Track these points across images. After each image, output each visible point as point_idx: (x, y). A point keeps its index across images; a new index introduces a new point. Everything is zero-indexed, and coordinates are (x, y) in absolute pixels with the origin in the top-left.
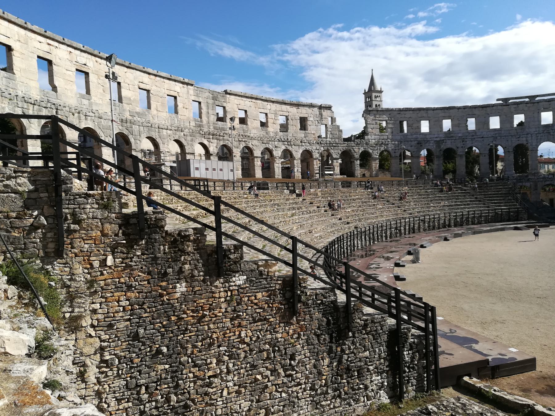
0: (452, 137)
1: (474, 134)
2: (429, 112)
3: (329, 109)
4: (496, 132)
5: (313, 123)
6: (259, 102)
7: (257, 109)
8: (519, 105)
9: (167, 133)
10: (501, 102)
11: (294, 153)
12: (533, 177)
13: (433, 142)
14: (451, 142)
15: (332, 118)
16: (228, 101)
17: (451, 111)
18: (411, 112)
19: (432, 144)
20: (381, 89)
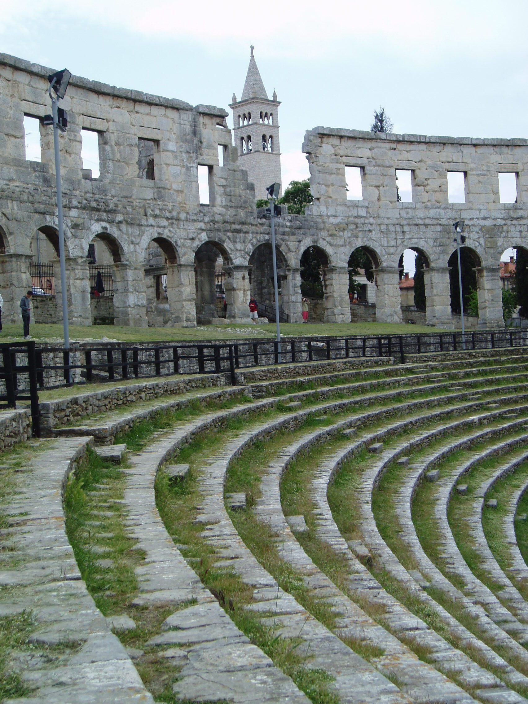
3: (218, 120)
5: (176, 157)
6: (23, 78)
7: (16, 100)
11: (127, 248)
15: (225, 147)
17: (518, 150)
18: (423, 147)
19: (476, 236)
20: (275, 96)
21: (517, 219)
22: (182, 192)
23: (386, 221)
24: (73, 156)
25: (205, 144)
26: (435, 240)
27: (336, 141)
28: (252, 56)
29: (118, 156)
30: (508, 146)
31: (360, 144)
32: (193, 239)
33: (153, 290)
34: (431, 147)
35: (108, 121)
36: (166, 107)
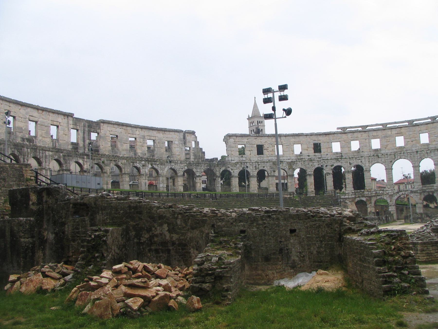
0: (302, 159)
1: (320, 157)
2: (282, 138)
4: (338, 155)
5: (178, 146)
6: (129, 128)
7: (127, 134)
8: (354, 133)
9: (49, 154)
10: (340, 130)
12: (368, 193)
13: (285, 163)
14: (301, 163)
16: (101, 128)
17: (301, 137)
18: (267, 138)
19: (285, 165)
21: (301, 159)
22: (179, 155)
23: (252, 161)
24: (144, 147)
25: (187, 141)
26: (270, 167)
27: (235, 138)
28: (255, 101)
29: (158, 146)
30: (297, 136)
31: (243, 138)
32: (182, 168)
33: (172, 183)
34: (270, 137)
35: (156, 137)
36: (175, 132)
